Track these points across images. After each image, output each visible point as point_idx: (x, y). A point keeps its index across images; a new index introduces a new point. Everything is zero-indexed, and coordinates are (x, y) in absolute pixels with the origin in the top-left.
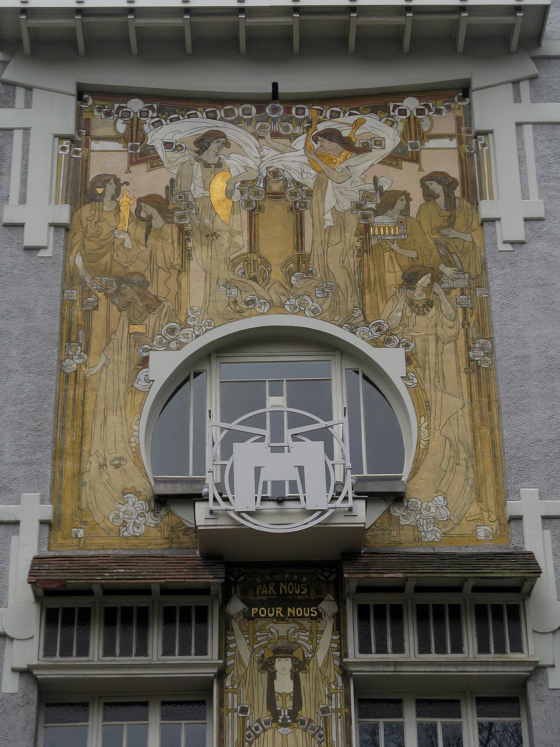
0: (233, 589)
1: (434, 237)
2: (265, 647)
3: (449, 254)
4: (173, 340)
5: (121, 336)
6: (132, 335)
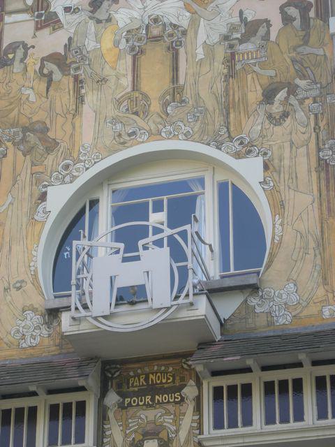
0: (110, 384)
1: (290, 55)
2: (135, 431)
3: (304, 69)
4: (67, 174)
5: (25, 177)
6: (34, 175)
